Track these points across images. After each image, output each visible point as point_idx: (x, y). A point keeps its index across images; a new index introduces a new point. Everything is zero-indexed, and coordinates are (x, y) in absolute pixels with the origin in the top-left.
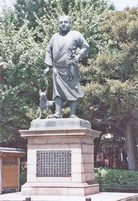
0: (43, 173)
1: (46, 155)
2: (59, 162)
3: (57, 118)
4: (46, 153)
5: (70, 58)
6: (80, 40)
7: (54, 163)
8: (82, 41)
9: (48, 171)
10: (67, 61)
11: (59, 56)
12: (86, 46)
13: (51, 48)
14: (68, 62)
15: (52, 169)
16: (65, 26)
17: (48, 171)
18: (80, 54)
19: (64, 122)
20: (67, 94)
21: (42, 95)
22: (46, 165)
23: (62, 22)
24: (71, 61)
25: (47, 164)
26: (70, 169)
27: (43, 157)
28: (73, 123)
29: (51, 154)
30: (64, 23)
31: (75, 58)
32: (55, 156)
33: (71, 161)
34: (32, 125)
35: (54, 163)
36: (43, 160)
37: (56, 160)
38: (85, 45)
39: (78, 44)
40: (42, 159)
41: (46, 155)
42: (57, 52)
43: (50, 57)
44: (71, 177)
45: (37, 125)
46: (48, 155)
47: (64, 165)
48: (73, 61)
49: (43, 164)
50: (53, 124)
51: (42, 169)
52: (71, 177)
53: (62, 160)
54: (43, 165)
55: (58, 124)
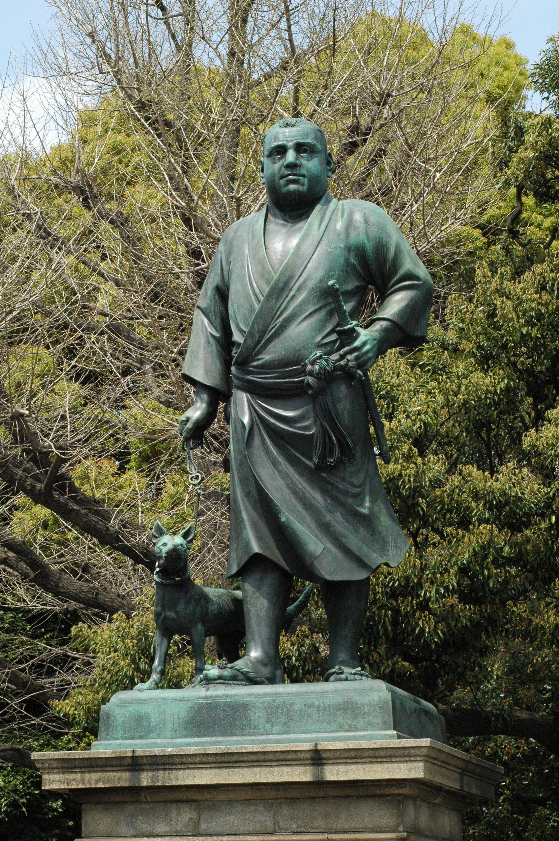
3: (252, 681)
5: (333, 337)
6: (381, 247)
8: (392, 254)
10: (312, 357)
11: (263, 333)
12: (417, 278)
13: (222, 293)
14: (318, 361)
16: (304, 171)
18: (384, 323)
20: (314, 543)
21: (170, 546)
23: (281, 150)
24: (335, 357)
28: (350, 710)
30: (291, 156)
31: (357, 343)
34: (106, 731)
38: (410, 276)
39: (374, 267)
42: (252, 309)
43: (212, 341)
45: (140, 725)
48: (342, 357)
50: (230, 718)
55: (258, 717)
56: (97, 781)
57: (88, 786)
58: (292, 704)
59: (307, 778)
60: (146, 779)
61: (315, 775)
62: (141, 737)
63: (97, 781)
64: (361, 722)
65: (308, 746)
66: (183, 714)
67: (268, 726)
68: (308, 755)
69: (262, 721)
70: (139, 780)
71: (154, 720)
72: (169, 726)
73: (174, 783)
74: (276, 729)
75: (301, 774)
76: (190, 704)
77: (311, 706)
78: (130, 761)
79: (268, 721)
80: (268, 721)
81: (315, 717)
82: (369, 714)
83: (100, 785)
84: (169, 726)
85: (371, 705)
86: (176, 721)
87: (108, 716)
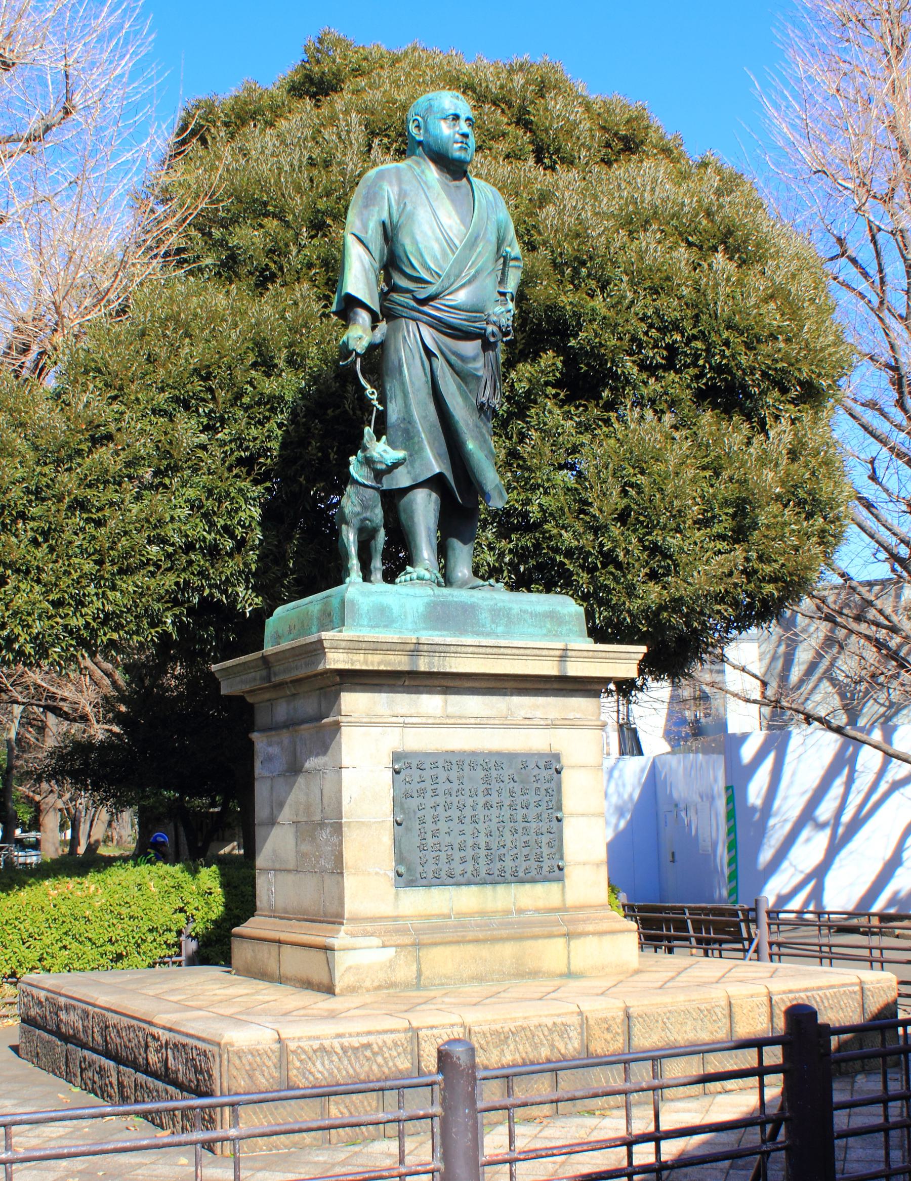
0: (430, 868)
1: (443, 775)
2: (506, 813)
4: (440, 764)
7: (481, 812)
9: (457, 855)
11: (458, 276)
15: (476, 846)
17: (457, 855)
19: (516, 609)
22: (443, 826)
25: (449, 819)
26: (557, 844)
27: (428, 785)
29: (466, 767)
32: (487, 780)
33: (560, 808)
35: (481, 812)
36: (429, 802)
37: (494, 799)
40: (422, 792)
41: (443, 775)
44: (560, 879)
46: (453, 775)
47: (534, 825)
49: (429, 820)
51: (422, 848)
52: (560, 879)
53: (519, 799)
54: (429, 827)
55: (485, 616)
56: (379, 664)
57: (371, 668)
58: (510, 609)
59: (554, 672)
60: (423, 665)
61: (560, 670)
62: (385, 626)
63: (379, 664)
64: (564, 629)
65: (561, 645)
66: (421, 609)
67: (493, 626)
68: (558, 653)
69: (488, 621)
70: (417, 666)
71: (396, 610)
72: (410, 619)
73: (454, 670)
74: (500, 629)
75: (549, 668)
76: (426, 600)
77: (526, 612)
78: (412, 647)
79: (493, 622)
80: (493, 622)
81: (530, 621)
82: (569, 622)
83: (382, 668)
84: (410, 619)
85: (570, 615)
86: (416, 614)
87: (352, 602)
